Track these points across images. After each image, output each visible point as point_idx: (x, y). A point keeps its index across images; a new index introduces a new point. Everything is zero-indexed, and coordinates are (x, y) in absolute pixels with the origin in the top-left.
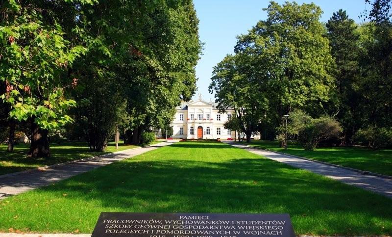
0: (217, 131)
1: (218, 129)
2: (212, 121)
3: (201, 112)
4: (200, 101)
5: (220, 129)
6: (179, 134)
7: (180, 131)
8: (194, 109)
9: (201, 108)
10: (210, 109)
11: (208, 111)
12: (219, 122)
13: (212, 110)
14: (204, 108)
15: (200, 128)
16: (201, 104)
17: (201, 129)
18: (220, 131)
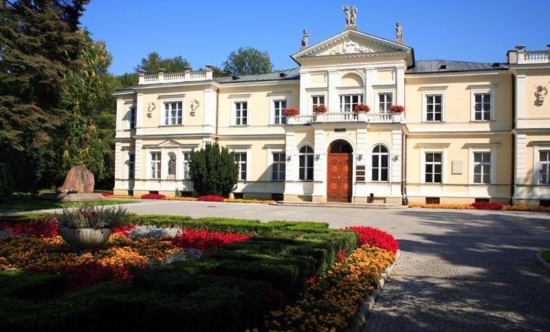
0: (429, 168)
1: (429, 157)
2: (397, 118)
3: (356, 84)
4: (352, 37)
5: (438, 157)
6: (269, 178)
7: (274, 167)
8: (327, 73)
9: (357, 66)
10: (395, 69)
11: (387, 78)
12: (435, 127)
13: (401, 74)
14: (368, 65)
15: (341, 149)
16: (352, 48)
17: (345, 156)
18: (439, 168)
